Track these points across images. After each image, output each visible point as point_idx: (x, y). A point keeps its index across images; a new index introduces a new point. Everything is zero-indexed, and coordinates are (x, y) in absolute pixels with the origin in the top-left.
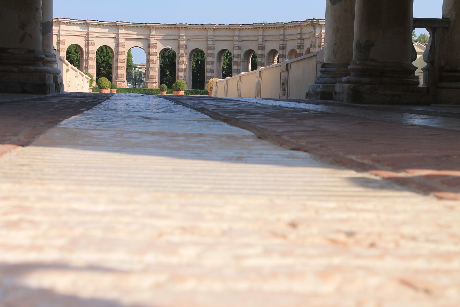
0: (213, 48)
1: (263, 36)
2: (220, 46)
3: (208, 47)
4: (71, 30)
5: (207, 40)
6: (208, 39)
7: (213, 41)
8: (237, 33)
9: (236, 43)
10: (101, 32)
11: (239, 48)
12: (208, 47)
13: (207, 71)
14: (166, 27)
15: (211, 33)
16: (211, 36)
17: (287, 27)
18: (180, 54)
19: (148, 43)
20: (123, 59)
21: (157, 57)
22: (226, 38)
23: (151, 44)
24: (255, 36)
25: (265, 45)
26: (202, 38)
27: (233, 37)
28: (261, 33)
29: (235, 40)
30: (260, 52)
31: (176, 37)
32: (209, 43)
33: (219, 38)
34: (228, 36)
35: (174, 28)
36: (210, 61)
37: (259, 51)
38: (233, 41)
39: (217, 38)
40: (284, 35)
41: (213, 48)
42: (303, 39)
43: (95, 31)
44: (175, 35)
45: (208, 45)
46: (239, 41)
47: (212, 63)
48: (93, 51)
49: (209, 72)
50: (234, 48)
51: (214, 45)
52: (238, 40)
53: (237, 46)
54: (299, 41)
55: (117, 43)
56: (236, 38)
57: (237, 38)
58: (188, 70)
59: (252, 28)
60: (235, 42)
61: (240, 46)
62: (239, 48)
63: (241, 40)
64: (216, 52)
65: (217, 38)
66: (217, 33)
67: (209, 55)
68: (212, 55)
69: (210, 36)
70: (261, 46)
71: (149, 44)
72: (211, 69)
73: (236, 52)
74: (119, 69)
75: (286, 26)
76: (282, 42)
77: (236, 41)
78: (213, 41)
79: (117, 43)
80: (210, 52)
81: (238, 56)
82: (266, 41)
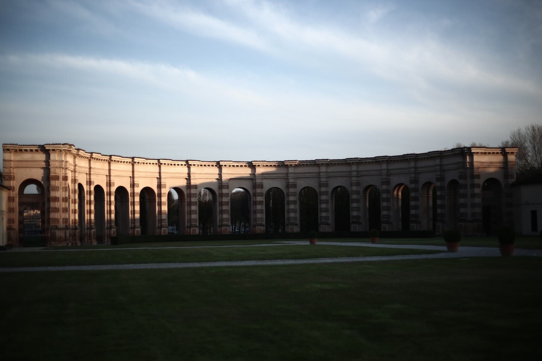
0: (326, 185)
1: (388, 170)
2: (334, 183)
3: (321, 185)
4: (172, 172)
5: (319, 177)
6: (320, 176)
7: (327, 177)
8: (354, 168)
9: (353, 179)
10: (202, 173)
11: (358, 184)
12: (321, 185)
13: (229, 212)
14: (269, 164)
15: (323, 169)
16: (324, 172)
17: (419, 158)
18: (290, 194)
19: (253, 183)
20: (227, 202)
21: (263, 198)
22: (341, 174)
23: (256, 184)
24: (376, 170)
25: (389, 179)
26: (313, 174)
27: (350, 172)
28: (412, 164)
29: (353, 175)
30: (384, 187)
31: (284, 175)
32: (322, 180)
33: (332, 174)
34: (344, 172)
35: (282, 165)
36: (324, 200)
37: (383, 186)
38: (350, 177)
39: (330, 174)
40: (416, 168)
41: (326, 185)
42: (444, 171)
43: (198, 173)
44: (282, 173)
45: (321, 183)
46: (357, 177)
47: (326, 202)
48: (195, 194)
49: (324, 211)
50: (352, 185)
51: (327, 182)
52: (356, 175)
53: (356, 182)
54: (439, 173)
55: (220, 184)
56: (354, 174)
57: (355, 173)
58: (298, 211)
59: (372, 162)
60: (353, 178)
61: (359, 182)
62: (358, 184)
63: (359, 175)
64: (330, 190)
65: (330, 174)
66: (331, 169)
67: (321, 193)
68: (326, 193)
69: (322, 172)
70: (385, 180)
71: (254, 184)
72: (326, 208)
73: (354, 188)
74: (224, 213)
75: (419, 157)
76: (413, 175)
77: (354, 177)
78: (327, 177)
79: (220, 184)
80: (323, 189)
81: (357, 192)
82: (391, 174)
